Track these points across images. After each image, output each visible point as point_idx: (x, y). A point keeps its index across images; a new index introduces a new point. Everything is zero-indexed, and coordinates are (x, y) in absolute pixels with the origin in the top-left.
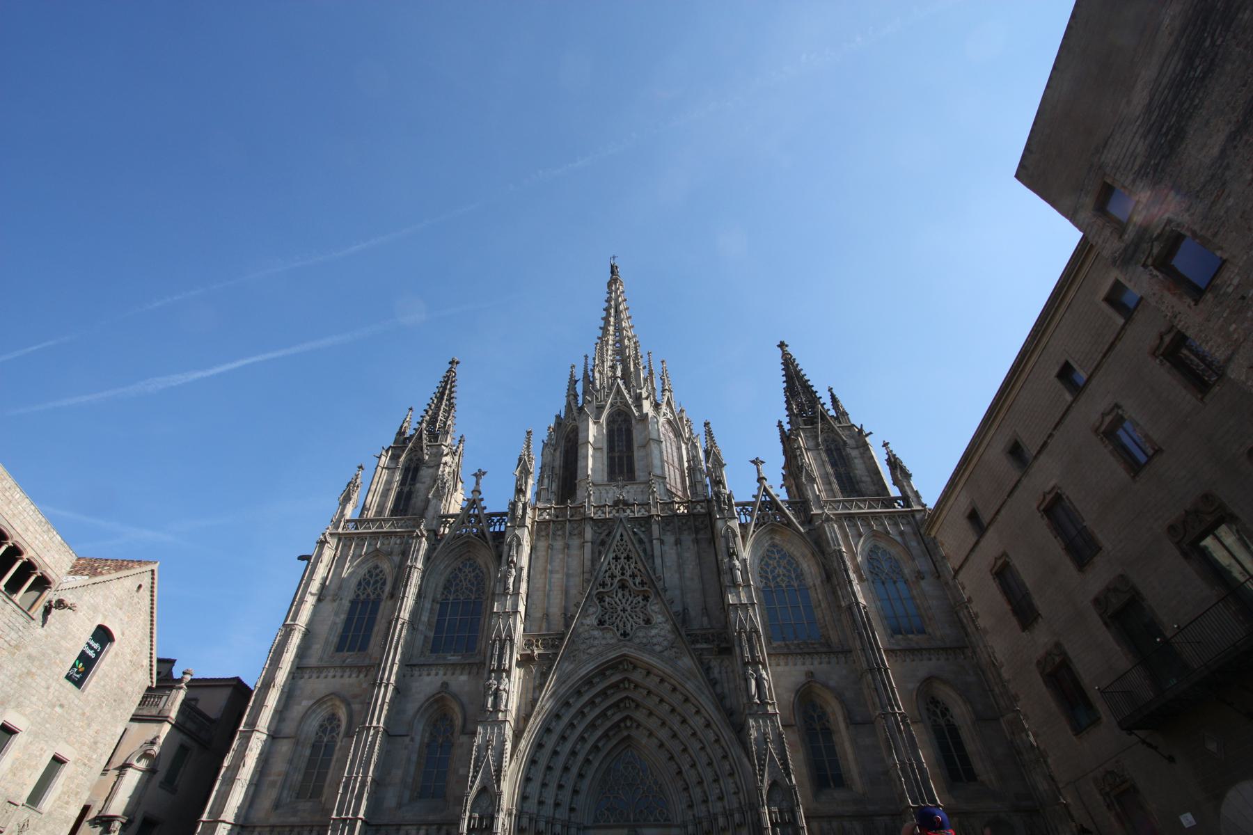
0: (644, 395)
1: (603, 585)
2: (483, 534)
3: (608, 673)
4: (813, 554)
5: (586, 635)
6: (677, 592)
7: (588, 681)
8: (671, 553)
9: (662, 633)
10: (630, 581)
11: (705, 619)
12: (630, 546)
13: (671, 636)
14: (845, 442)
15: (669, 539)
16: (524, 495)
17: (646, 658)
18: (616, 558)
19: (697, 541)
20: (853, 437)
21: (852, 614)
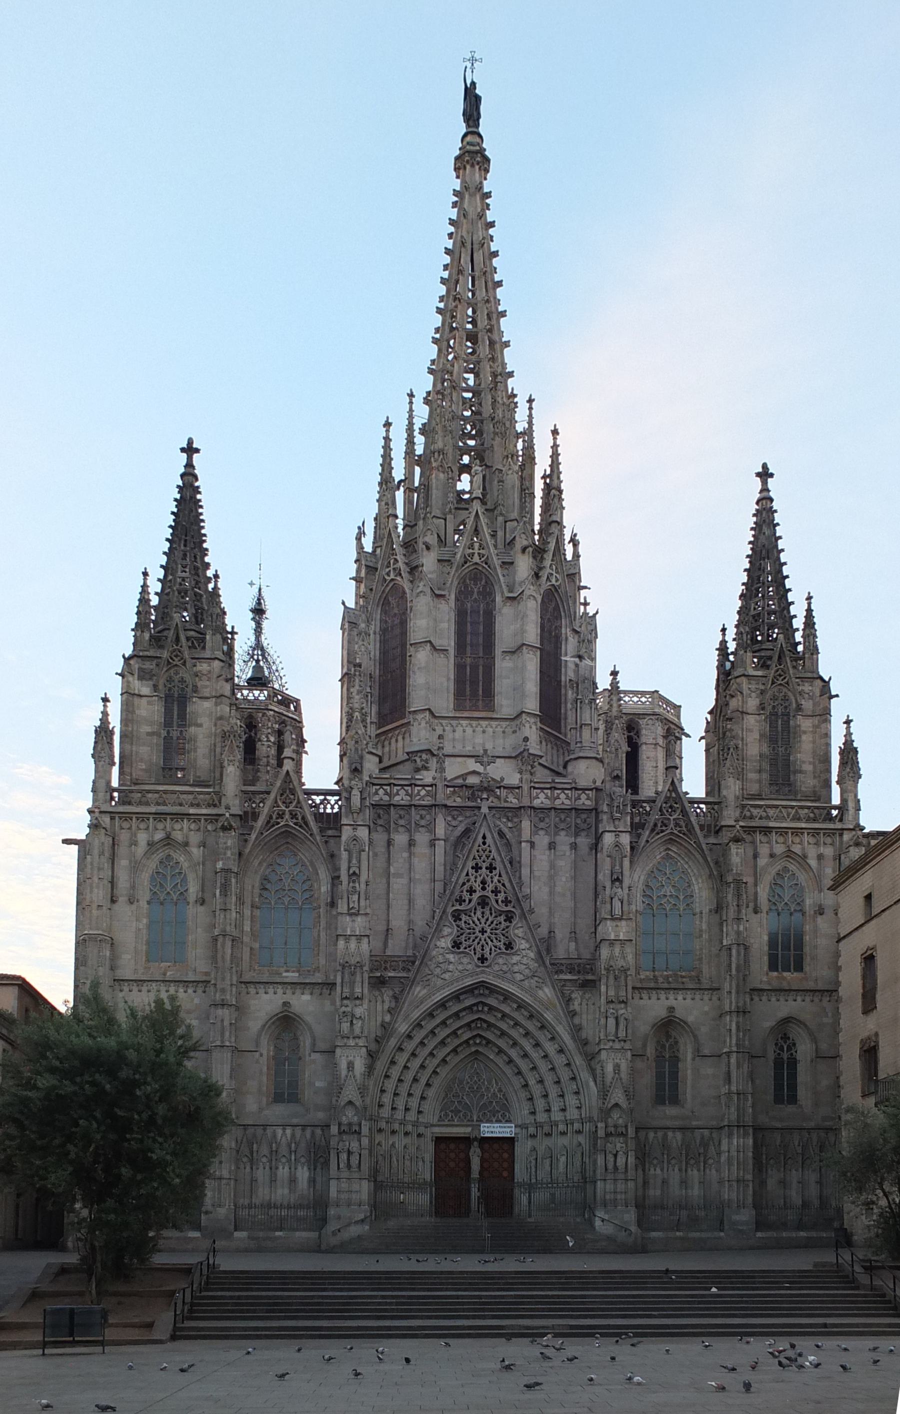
0: (518, 545)
1: (461, 901)
2: (306, 823)
3: (462, 997)
4: (710, 875)
5: (441, 959)
6: (545, 910)
7: (442, 1005)
8: (542, 857)
9: (525, 961)
10: (492, 896)
11: (573, 945)
12: (494, 853)
13: (534, 965)
14: (799, 708)
15: (542, 840)
16: (361, 779)
17: (505, 986)
18: (477, 868)
19: (574, 846)
20: (811, 698)
21: (731, 956)
